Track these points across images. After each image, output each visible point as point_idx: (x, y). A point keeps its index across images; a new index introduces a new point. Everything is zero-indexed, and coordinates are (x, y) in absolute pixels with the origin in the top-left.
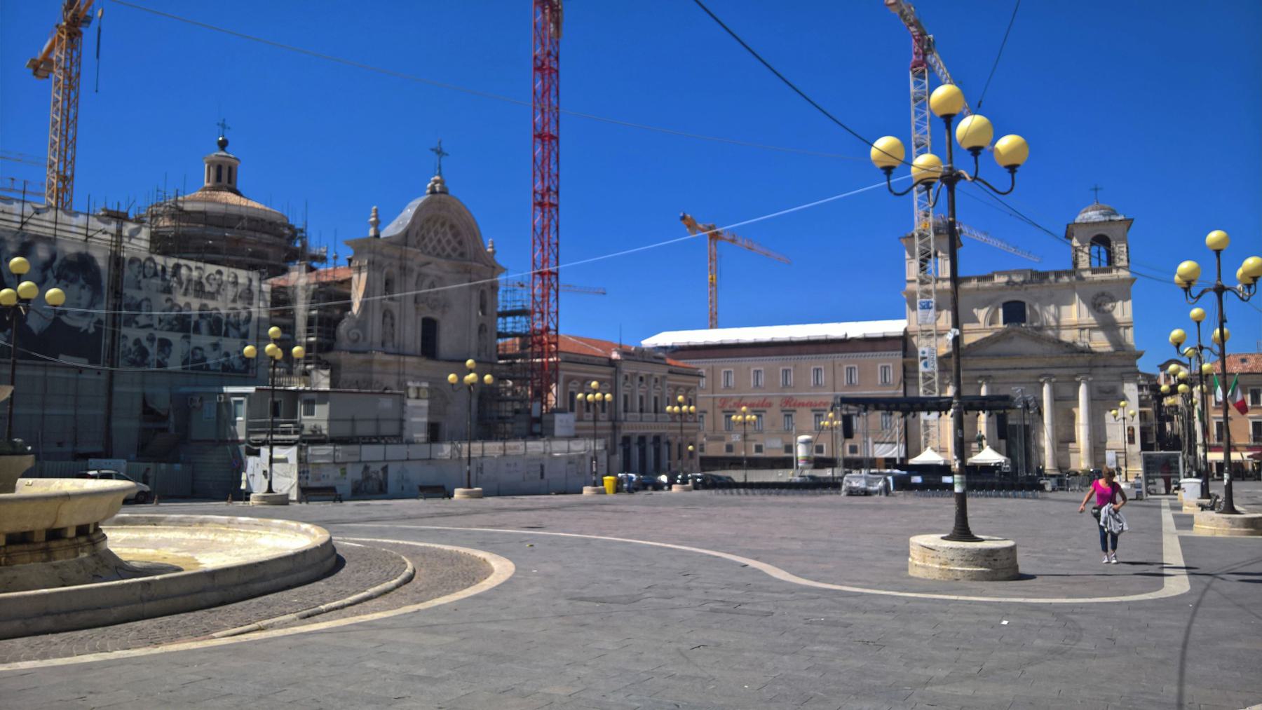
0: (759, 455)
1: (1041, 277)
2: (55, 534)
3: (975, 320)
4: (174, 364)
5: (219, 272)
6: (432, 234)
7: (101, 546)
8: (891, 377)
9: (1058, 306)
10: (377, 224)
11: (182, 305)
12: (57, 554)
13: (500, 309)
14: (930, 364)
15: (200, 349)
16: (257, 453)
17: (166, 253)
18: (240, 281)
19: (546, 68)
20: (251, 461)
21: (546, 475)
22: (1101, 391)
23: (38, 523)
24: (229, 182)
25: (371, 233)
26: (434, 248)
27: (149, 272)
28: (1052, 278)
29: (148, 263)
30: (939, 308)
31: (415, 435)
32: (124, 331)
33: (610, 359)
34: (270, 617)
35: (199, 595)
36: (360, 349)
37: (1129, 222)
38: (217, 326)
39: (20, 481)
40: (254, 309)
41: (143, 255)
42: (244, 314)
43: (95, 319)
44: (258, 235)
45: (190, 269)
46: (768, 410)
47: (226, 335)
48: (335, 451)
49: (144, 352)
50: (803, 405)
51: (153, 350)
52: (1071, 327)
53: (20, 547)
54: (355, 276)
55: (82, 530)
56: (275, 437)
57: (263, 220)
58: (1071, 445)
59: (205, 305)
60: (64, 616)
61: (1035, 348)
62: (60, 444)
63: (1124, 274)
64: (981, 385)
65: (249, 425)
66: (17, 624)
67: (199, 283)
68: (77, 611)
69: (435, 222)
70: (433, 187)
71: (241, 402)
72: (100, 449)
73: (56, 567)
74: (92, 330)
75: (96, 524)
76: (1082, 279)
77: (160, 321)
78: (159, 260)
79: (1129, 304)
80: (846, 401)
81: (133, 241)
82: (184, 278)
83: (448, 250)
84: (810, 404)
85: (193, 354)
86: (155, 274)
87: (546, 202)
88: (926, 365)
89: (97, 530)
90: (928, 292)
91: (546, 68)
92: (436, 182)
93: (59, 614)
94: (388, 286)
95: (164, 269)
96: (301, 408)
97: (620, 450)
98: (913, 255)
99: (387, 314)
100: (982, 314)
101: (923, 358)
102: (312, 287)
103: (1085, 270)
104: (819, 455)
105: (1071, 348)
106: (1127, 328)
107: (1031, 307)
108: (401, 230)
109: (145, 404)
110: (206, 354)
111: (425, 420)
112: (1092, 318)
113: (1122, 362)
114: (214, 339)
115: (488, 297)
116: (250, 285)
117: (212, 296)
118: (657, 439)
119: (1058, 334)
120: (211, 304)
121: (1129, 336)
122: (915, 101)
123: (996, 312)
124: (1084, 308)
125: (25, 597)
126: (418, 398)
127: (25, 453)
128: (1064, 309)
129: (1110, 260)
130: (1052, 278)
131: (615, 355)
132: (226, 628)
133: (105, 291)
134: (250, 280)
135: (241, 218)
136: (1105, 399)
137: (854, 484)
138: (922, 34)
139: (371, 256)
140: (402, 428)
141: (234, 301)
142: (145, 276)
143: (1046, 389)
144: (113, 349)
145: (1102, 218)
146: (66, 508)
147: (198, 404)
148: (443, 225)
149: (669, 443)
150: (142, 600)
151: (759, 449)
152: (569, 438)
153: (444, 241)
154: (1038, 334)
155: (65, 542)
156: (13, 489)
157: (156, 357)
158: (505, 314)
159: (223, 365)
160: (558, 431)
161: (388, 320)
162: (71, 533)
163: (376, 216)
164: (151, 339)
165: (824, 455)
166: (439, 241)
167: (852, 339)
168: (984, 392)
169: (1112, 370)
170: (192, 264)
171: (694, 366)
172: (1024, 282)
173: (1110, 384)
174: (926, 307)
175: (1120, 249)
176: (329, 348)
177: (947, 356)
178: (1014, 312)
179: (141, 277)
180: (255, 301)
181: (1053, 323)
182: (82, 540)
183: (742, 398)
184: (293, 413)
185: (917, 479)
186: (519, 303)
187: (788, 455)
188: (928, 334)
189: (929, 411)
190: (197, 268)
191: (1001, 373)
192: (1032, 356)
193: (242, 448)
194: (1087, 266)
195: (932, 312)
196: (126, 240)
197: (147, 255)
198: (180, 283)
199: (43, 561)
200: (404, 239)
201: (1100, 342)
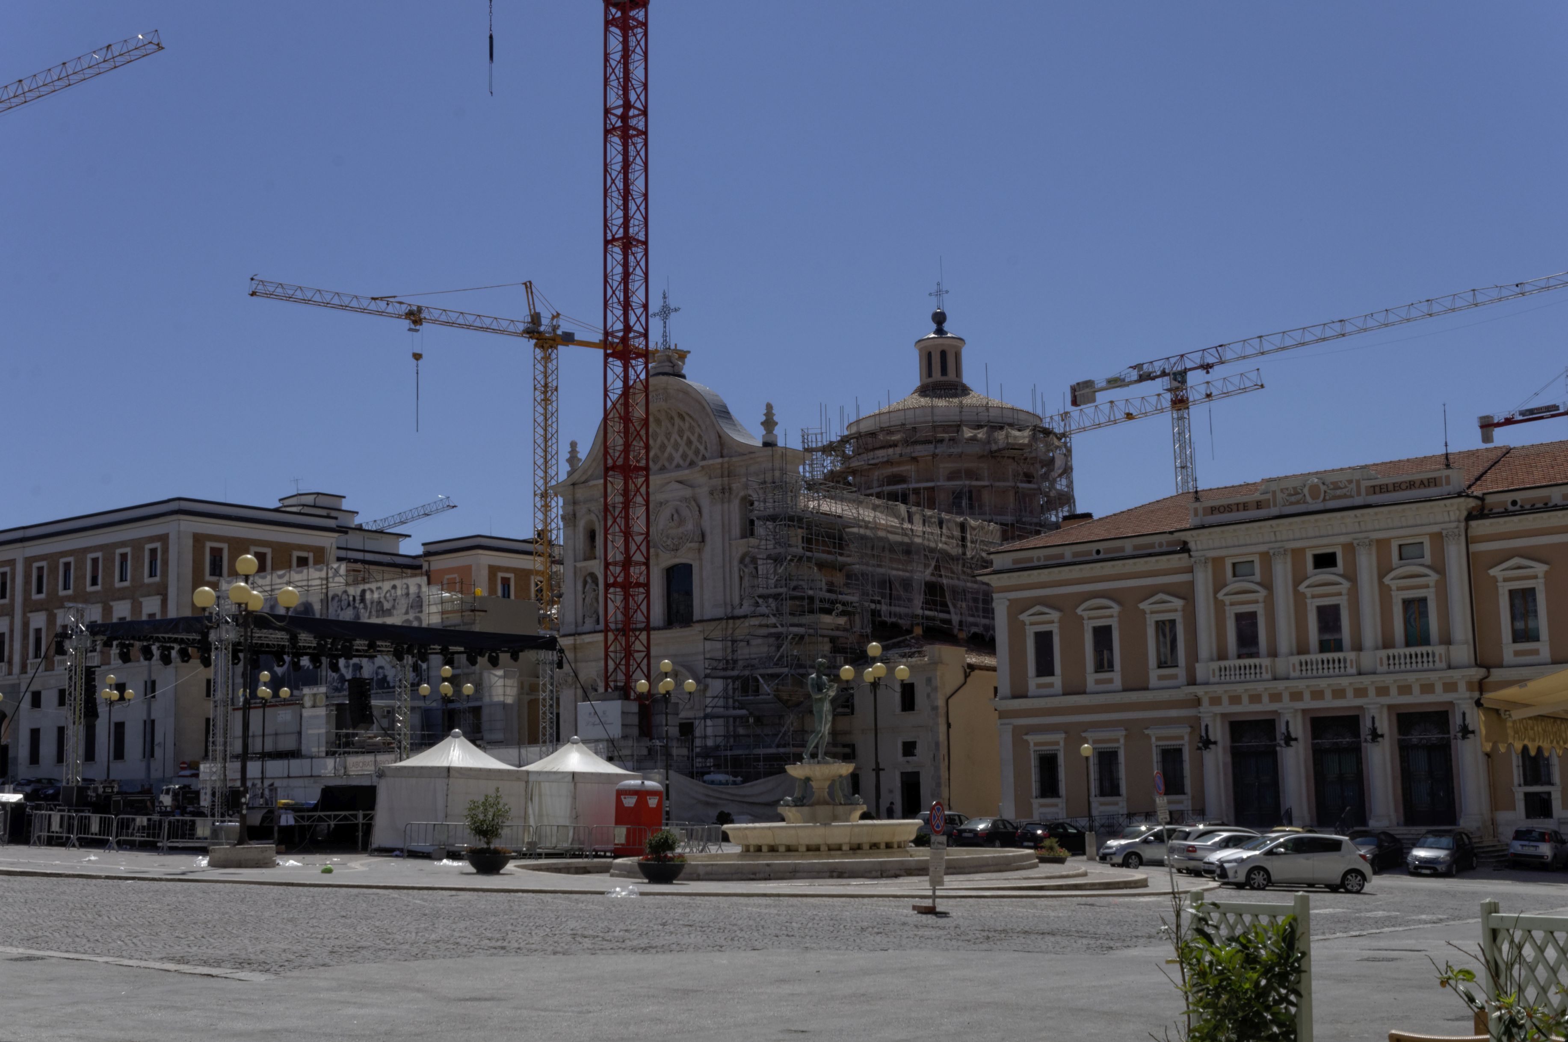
5: (394, 587)
6: (675, 436)
26: (684, 456)
27: (344, 603)
45: (372, 591)
67: (379, 603)
85: (377, 674)
111: (323, 731)
126: (314, 706)
134: (419, 586)
140: (300, 743)
141: (407, 613)
166: (689, 442)
170: (373, 586)
197: (343, 588)
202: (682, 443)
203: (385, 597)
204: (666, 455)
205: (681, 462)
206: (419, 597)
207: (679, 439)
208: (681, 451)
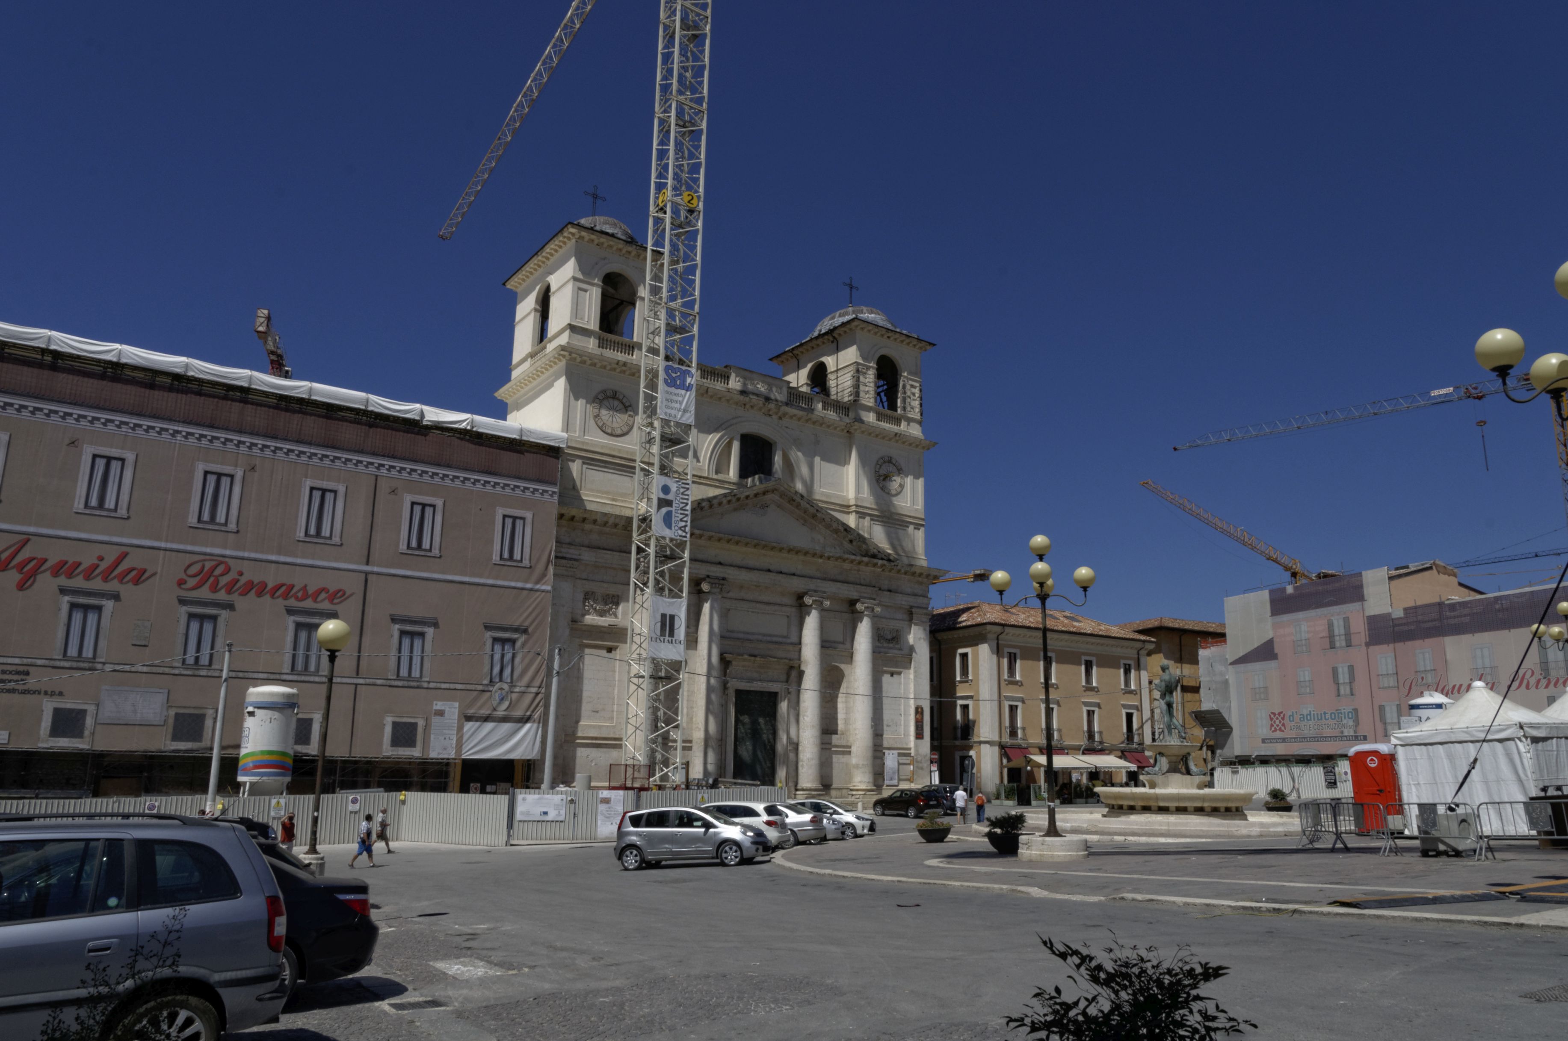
0: (64, 743)
8: (523, 549)
14: (676, 517)
46: (126, 590)
50: (261, 589)
52: (845, 508)
61: (799, 536)
84: (284, 590)
88: (667, 520)
104: (301, 749)
106: (917, 527)
123: (729, 445)
178: (756, 455)
191: (744, 576)
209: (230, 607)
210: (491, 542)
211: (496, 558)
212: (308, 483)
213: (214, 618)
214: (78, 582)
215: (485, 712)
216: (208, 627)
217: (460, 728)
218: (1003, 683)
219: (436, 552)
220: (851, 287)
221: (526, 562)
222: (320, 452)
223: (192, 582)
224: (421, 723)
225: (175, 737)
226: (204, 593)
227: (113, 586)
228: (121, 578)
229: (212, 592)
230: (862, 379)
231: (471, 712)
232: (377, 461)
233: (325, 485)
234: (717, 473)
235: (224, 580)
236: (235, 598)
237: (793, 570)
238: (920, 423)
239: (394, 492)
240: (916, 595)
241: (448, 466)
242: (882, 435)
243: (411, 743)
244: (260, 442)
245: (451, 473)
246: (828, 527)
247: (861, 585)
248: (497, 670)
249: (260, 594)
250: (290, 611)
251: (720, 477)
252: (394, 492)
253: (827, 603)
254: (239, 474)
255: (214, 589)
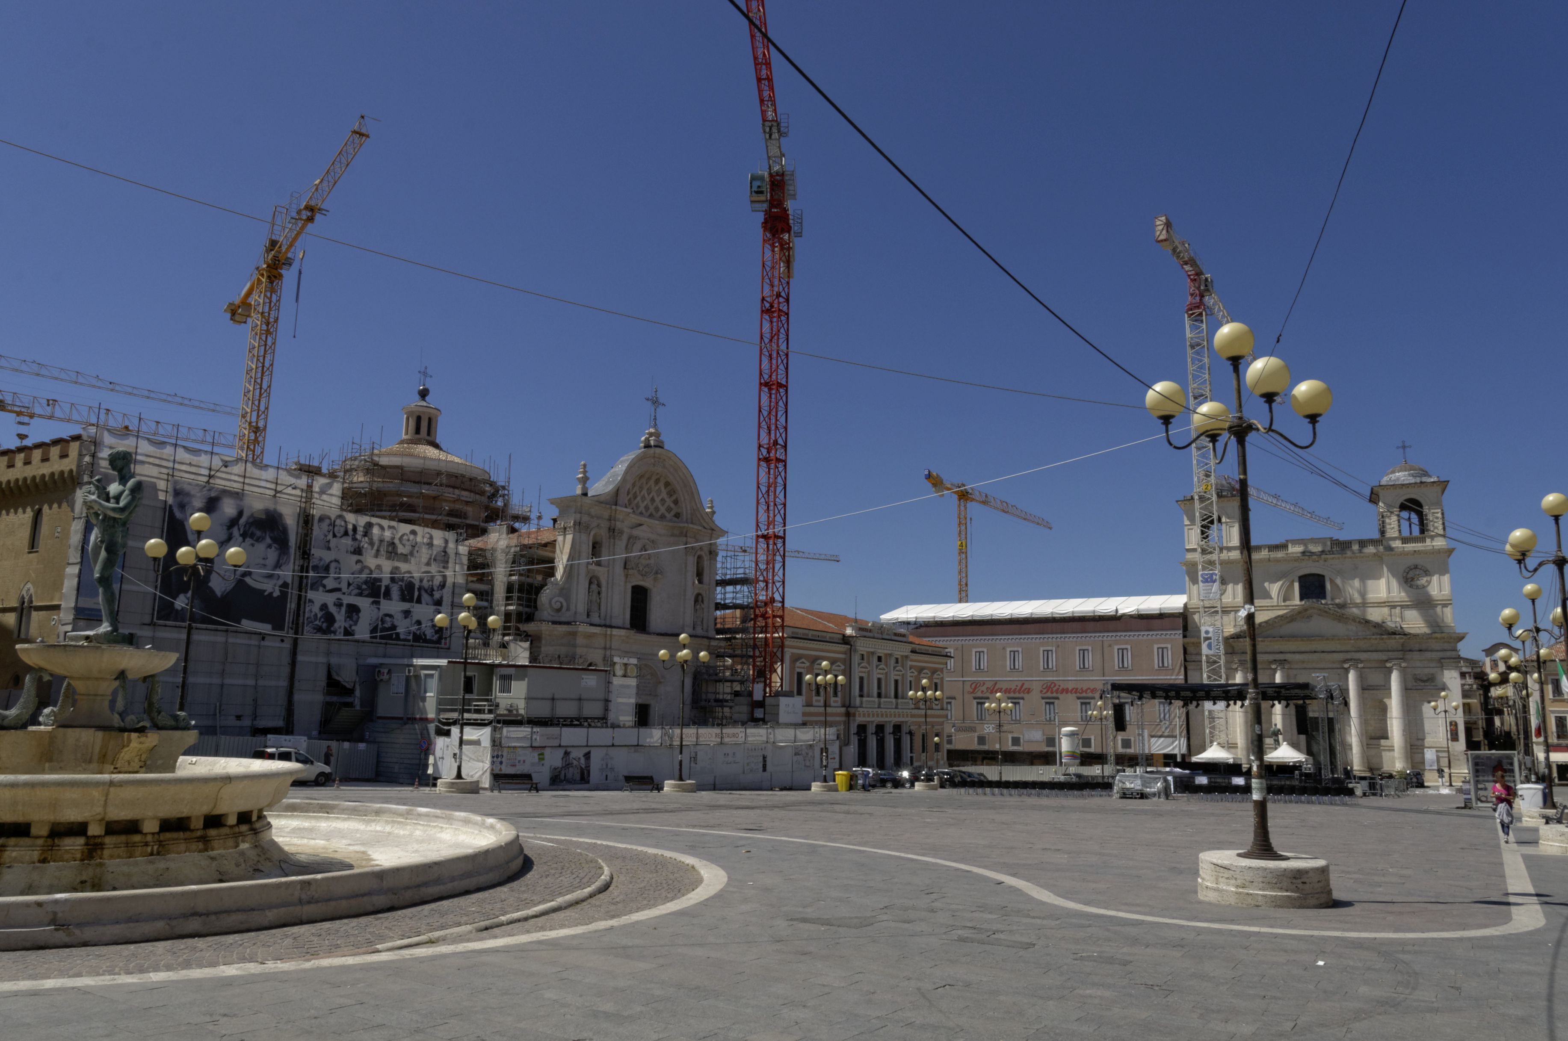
1: (1344, 546)
2: (214, 821)
3: (1267, 595)
4: (362, 632)
5: (414, 533)
6: (644, 492)
7: (264, 836)
8: (1168, 661)
9: (1364, 579)
10: (584, 480)
11: (373, 567)
12: (215, 844)
13: (718, 578)
14: (1214, 644)
15: (390, 616)
16: (447, 734)
17: (358, 510)
18: (436, 542)
19: (775, 310)
20: (440, 743)
21: (769, 768)
22: (1417, 679)
23: (195, 808)
24: (429, 434)
25: (579, 491)
26: (647, 508)
27: (339, 531)
28: (1356, 547)
29: (338, 522)
30: (1224, 582)
31: (621, 718)
32: (311, 595)
33: (844, 636)
34: (442, 928)
35: (365, 899)
36: (563, 619)
37: (1443, 485)
38: (410, 592)
39: (181, 758)
40: (449, 573)
41: (334, 513)
42: (438, 580)
43: (281, 582)
44: (457, 492)
45: (382, 528)
46: (1025, 696)
47: (419, 601)
48: (532, 733)
49: (330, 619)
50: (1066, 691)
51: (340, 617)
53: (175, 835)
54: (560, 539)
55: (244, 818)
56: (466, 716)
57: (463, 476)
58: (1383, 742)
59: (397, 568)
60: (213, 917)
61: (1340, 629)
62: (239, 718)
63: (1440, 543)
64: (1275, 671)
65: (440, 702)
66: (160, 925)
68: (228, 912)
69: (649, 479)
70: (647, 440)
71: (432, 676)
72: (280, 723)
73: (213, 859)
74: (276, 594)
75: (260, 811)
76: (1391, 549)
77: (349, 584)
78: (351, 518)
79: (1446, 578)
80: (1116, 687)
81: (324, 497)
82: (376, 539)
83: (663, 510)
84: (1075, 691)
86: (346, 533)
87: (773, 457)
88: (1210, 647)
89: (261, 817)
90: (1211, 563)
91: (775, 310)
92: (651, 435)
93: (207, 914)
94: (596, 548)
95: (355, 529)
96: (497, 684)
97: (854, 740)
98: (1192, 520)
99: (593, 581)
100: (1274, 589)
101: (1206, 639)
102: (513, 550)
103: (1394, 539)
104: (1087, 750)
105: (1380, 629)
106: (1445, 606)
107: (1332, 582)
108: (611, 487)
109: (329, 675)
110: (396, 623)
111: (633, 701)
112: (1403, 594)
113: (1441, 645)
114: (406, 606)
115: (706, 563)
116: (445, 547)
117: (405, 558)
118: (897, 728)
119: (1364, 612)
120: (404, 567)
121: (1448, 616)
122: (1192, 347)
124: (1394, 583)
125: (172, 894)
126: (625, 676)
127: (187, 728)
128: (1370, 583)
129: (1423, 529)
130: (1356, 547)
131: (849, 631)
132: (392, 939)
133: (292, 551)
134: (446, 542)
135: (439, 473)
136: (1422, 687)
137: (1128, 785)
138: (1199, 274)
139: (578, 516)
140: (606, 709)
141: (428, 564)
142: (334, 536)
143: (1352, 676)
144: (298, 615)
145: (1412, 480)
146: (227, 790)
147: (385, 677)
148: (657, 482)
149: (911, 733)
150: (301, 902)
151: (1016, 741)
152: (796, 725)
153: (658, 500)
154: (1340, 612)
155: (224, 831)
156: (172, 768)
157: (343, 624)
158: (724, 583)
159: (415, 634)
160: (783, 717)
161: (594, 587)
162: (232, 820)
163: (585, 472)
164: (339, 605)
165: (1092, 750)
166: (653, 500)
167: (1123, 615)
168: (1278, 679)
169: (1428, 655)
170: (385, 523)
171: (941, 644)
172: (1323, 552)
173: (1426, 671)
174: (1209, 580)
175: (1434, 516)
176: (530, 618)
177: (1237, 636)
178: (1313, 587)
179: (330, 536)
180: (450, 565)
181: (1358, 600)
182: (244, 828)
183: (996, 683)
184: (488, 690)
185: (1202, 780)
186: (741, 571)
187: (1050, 749)
188: (1212, 611)
189: (1215, 699)
190: (390, 527)
191: (1298, 657)
192: (1333, 638)
193: (432, 727)
194: (1396, 534)
195: (1216, 587)
196: (316, 495)
197: (338, 512)
198: (372, 544)
199: (200, 851)
200: (614, 499)
201: (1414, 622)
202: (648, 499)
203: (401, 539)
204: (636, 501)
205: (644, 512)
206: (445, 552)
207: (646, 495)
208: (645, 503)
209: (1057, 698)
210: (1153, 660)
211: (1156, 667)
212: (1078, 648)
213: (1053, 703)
214: (1012, 695)
215: (1160, 733)
216: (1052, 706)
217: (1149, 741)
218: (1547, 702)
219: (1130, 668)
220: (1404, 447)
221: (1170, 667)
222: (1080, 635)
223: (1045, 691)
224: (1132, 739)
225: (1048, 746)
226: (1049, 694)
227: (1021, 695)
228: (1023, 692)
229: (1052, 695)
230: (1387, 521)
231: (1153, 734)
232: (1102, 634)
233: (1084, 648)
234: (1284, 601)
235: (1055, 689)
236: (1059, 695)
237: (1333, 649)
238: (1444, 536)
239: (1110, 646)
240: (1445, 650)
241: (1131, 631)
242: (1404, 554)
243: (1130, 747)
244: (1059, 636)
245: (1132, 633)
246: (1354, 620)
247: (1389, 651)
248: (1162, 716)
249: (1067, 692)
250: (1078, 698)
251: (1288, 603)
252: (1110, 646)
253: (1360, 665)
254: (1054, 649)
255: (1052, 693)
